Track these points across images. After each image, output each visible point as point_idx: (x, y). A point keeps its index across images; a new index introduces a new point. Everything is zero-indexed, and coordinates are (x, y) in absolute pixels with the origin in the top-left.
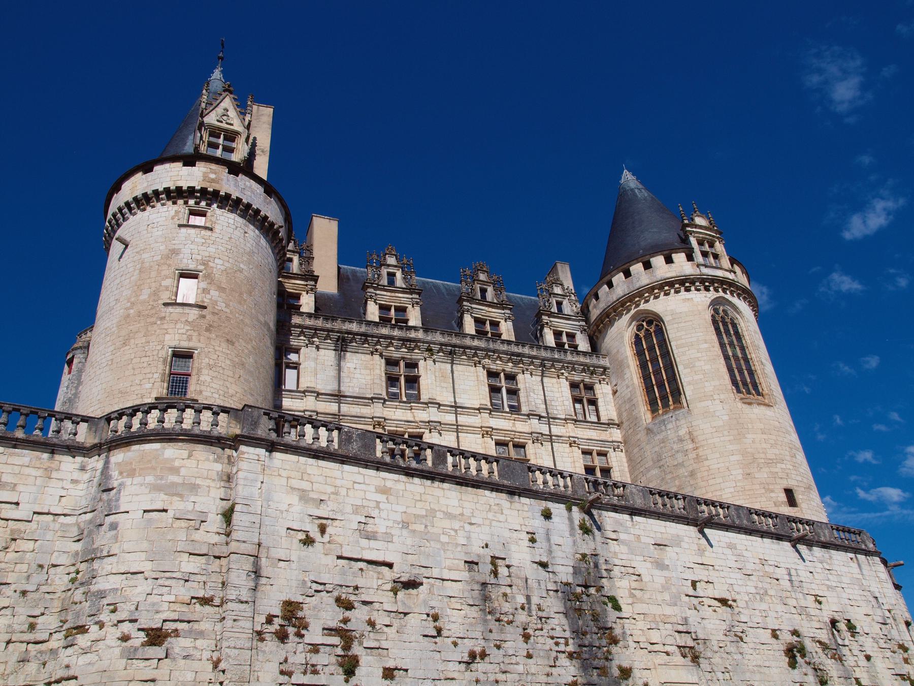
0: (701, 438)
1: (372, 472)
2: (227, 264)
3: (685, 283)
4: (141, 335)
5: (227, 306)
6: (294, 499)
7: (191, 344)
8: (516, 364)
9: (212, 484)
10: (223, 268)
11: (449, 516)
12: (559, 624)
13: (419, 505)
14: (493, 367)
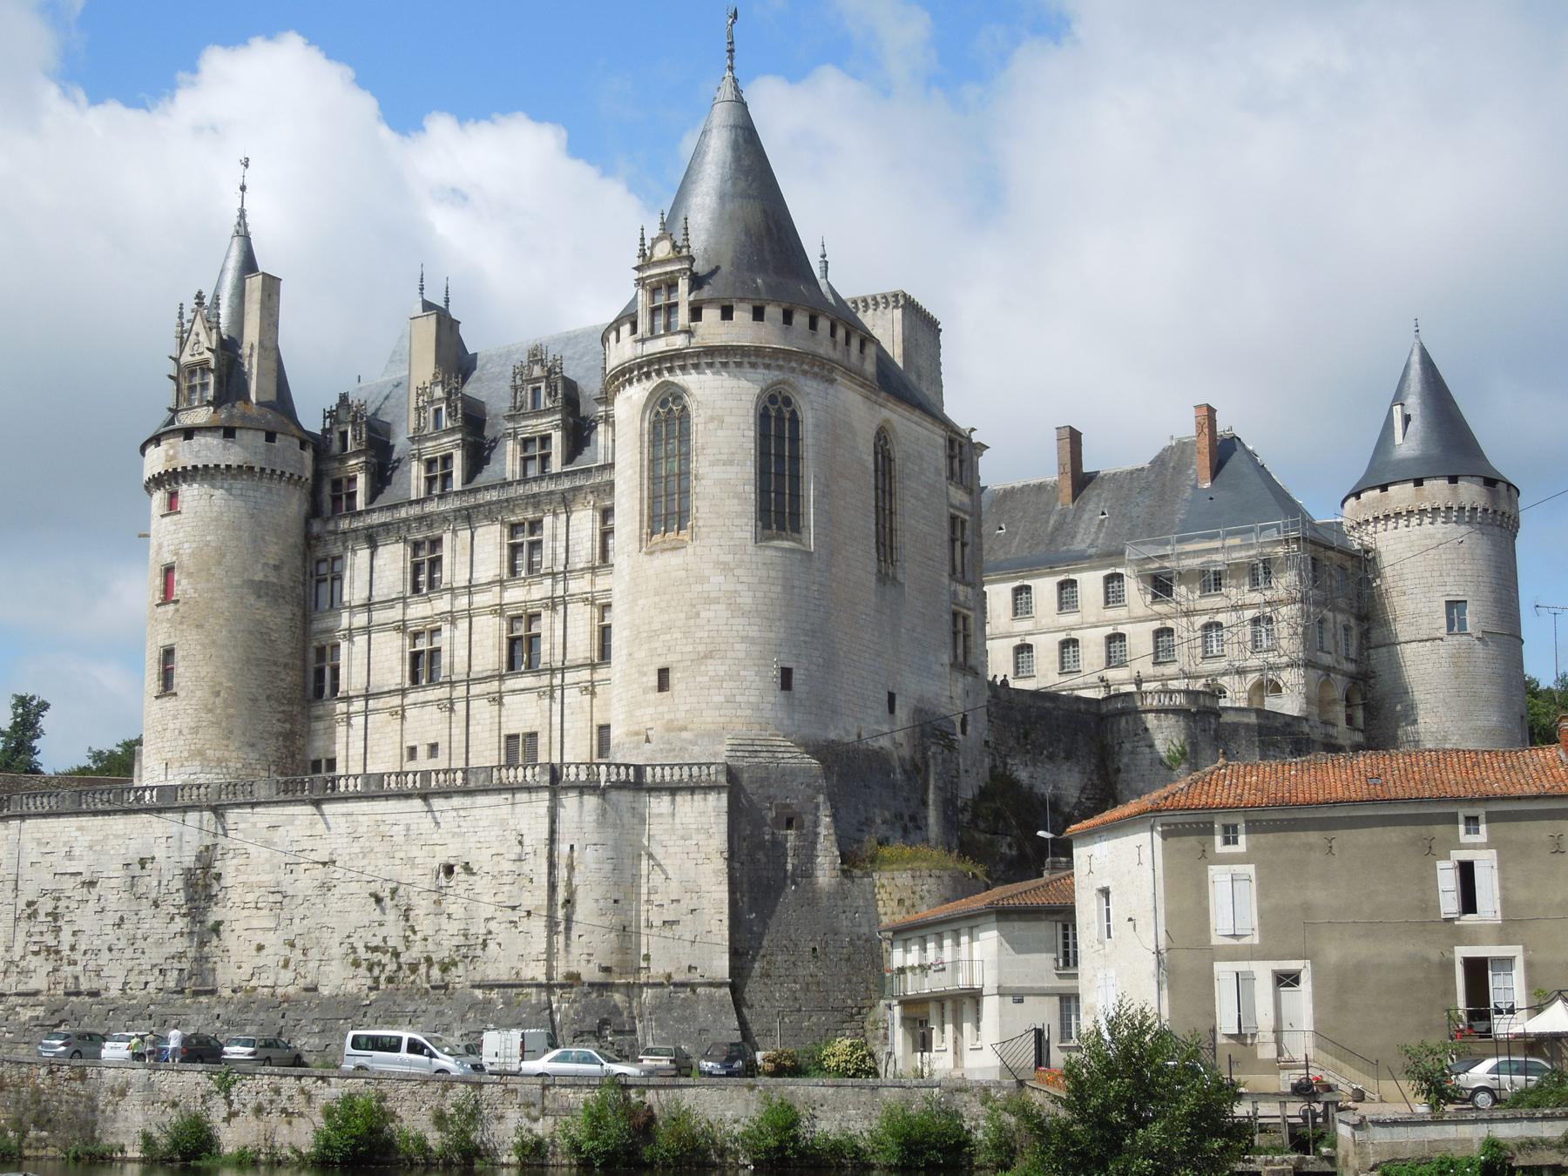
8: (537, 506)
12: (180, 898)
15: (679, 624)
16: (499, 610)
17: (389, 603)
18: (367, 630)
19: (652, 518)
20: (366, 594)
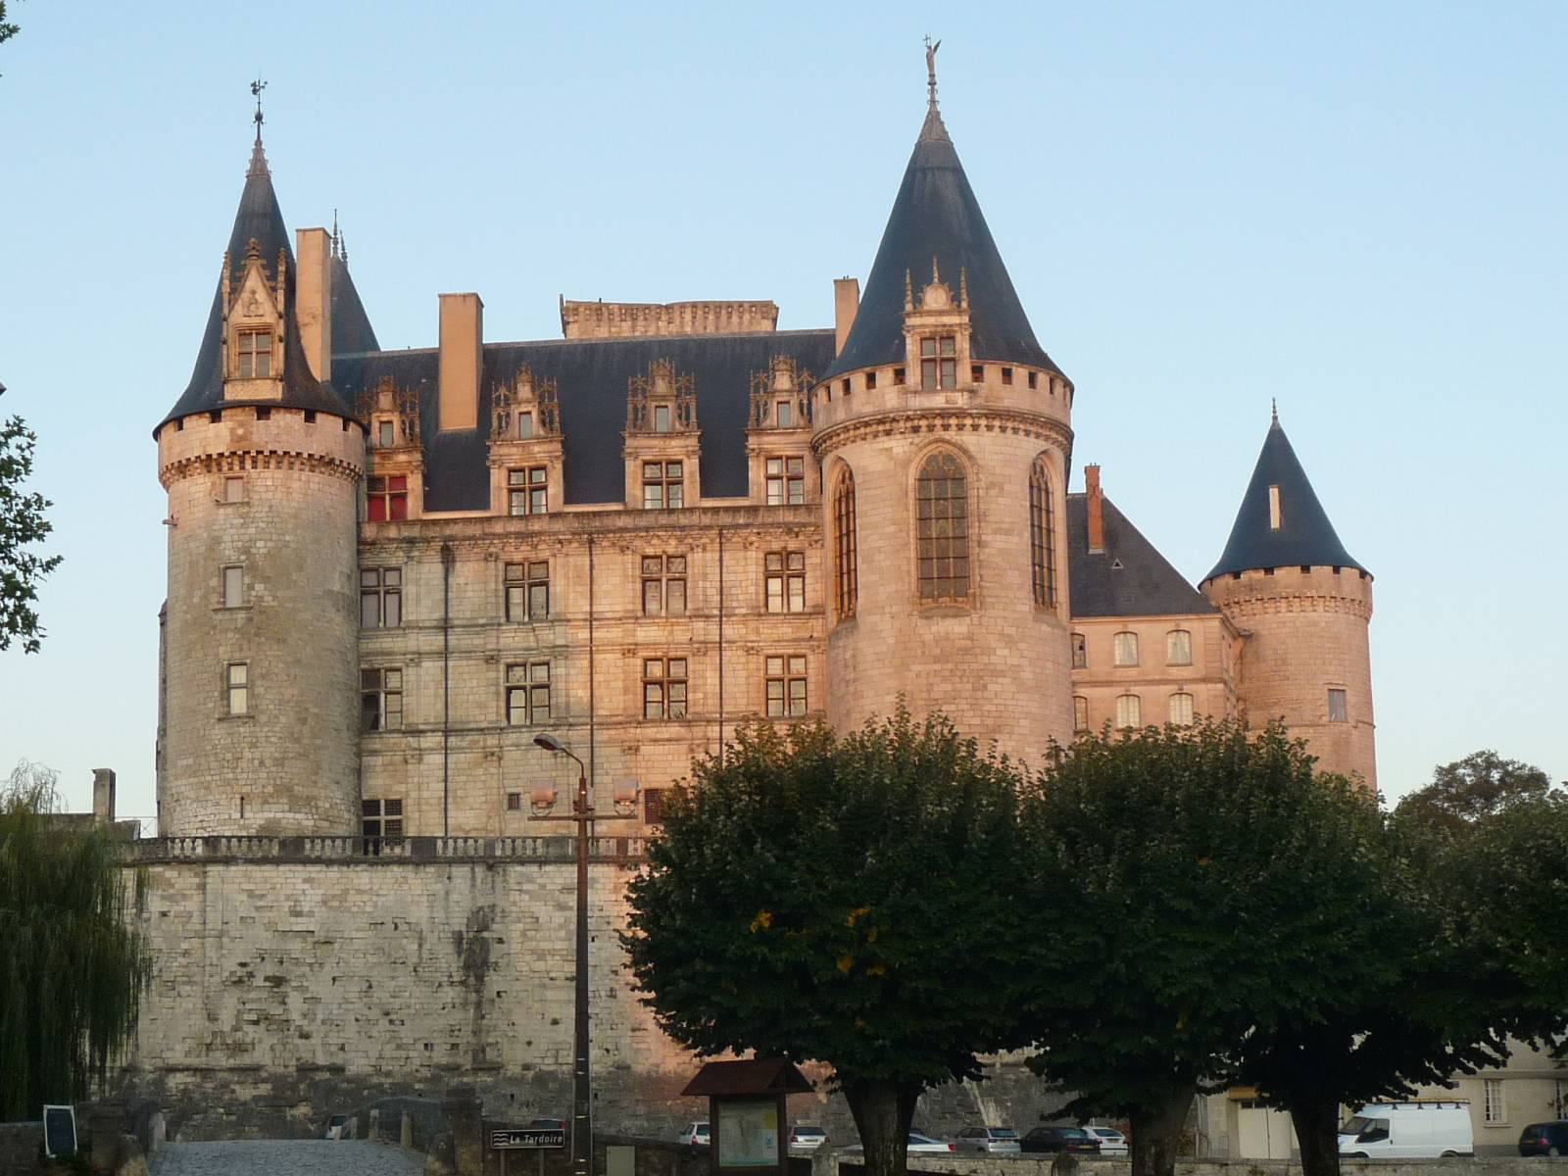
0: (861, 667)
1: (299, 868)
2: (270, 544)
3: (884, 423)
4: (199, 647)
5: (275, 598)
6: (244, 897)
7: (243, 654)
9: (193, 892)
10: (265, 551)
11: (360, 892)
13: (336, 887)
14: (650, 551)
15: (967, 694)
16: (630, 651)
17: (471, 627)
18: (445, 654)
19: (925, 579)
20: (439, 614)
